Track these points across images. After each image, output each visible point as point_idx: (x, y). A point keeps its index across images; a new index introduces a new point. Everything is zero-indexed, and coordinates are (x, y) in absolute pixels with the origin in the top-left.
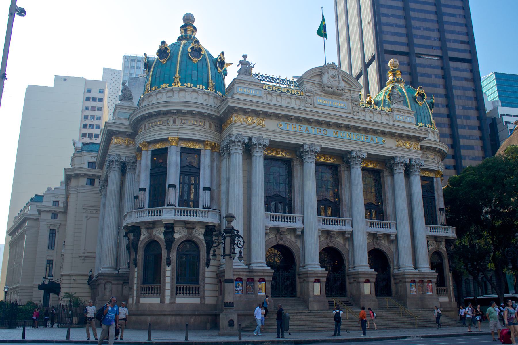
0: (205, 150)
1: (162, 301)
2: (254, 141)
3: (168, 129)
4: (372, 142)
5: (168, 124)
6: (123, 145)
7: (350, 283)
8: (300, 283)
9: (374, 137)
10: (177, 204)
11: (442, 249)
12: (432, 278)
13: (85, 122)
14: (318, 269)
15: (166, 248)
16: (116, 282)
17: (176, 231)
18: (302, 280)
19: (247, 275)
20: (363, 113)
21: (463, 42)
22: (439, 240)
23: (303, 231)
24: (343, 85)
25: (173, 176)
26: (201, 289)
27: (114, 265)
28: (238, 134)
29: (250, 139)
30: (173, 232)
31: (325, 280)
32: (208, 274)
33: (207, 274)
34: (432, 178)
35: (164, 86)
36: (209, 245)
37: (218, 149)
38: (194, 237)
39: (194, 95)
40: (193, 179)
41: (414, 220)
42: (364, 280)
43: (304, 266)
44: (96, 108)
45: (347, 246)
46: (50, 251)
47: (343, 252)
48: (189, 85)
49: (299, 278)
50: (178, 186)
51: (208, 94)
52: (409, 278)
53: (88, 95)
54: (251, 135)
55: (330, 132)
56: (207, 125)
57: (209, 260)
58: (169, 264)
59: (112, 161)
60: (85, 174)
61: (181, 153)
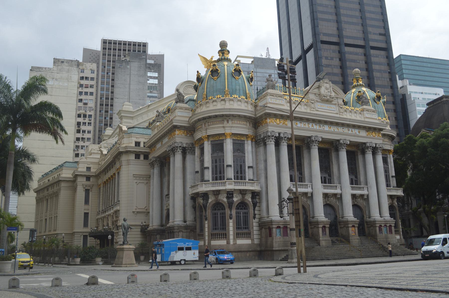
0: (247, 140)
1: (228, 243)
2: (282, 135)
3: (224, 127)
5: (223, 123)
6: (183, 135)
7: (341, 228)
8: (311, 228)
9: (353, 130)
10: (233, 178)
12: (392, 223)
13: (80, 98)
14: (323, 219)
15: (229, 207)
16: (185, 231)
17: (234, 196)
18: (313, 227)
19: (283, 224)
20: (345, 113)
21: (380, 34)
22: (393, 197)
23: (312, 194)
24: (333, 94)
25: (229, 159)
26: (252, 234)
27: (182, 219)
28: (273, 131)
29: (279, 134)
30: (233, 197)
31: (328, 226)
32: (255, 224)
33: (255, 224)
35: (219, 96)
36: (255, 205)
37: (255, 140)
39: (239, 103)
41: (379, 185)
42: (351, 225)
43: (313, 217)
44: (89, 86)
45: (337, 203)
46: (87, 207)
47: (336, 207)
48: (235, 96)
49: (311, 225)
50: (233, 166)
51: (247, 102)
53: (82, 75)
54: (280, 131)
55: (326, 128)
56: (248, 124)
57: (255, 215)
58: (231, 218)
59: (177, 147)
60: (134, 151)
61: (233, 143)
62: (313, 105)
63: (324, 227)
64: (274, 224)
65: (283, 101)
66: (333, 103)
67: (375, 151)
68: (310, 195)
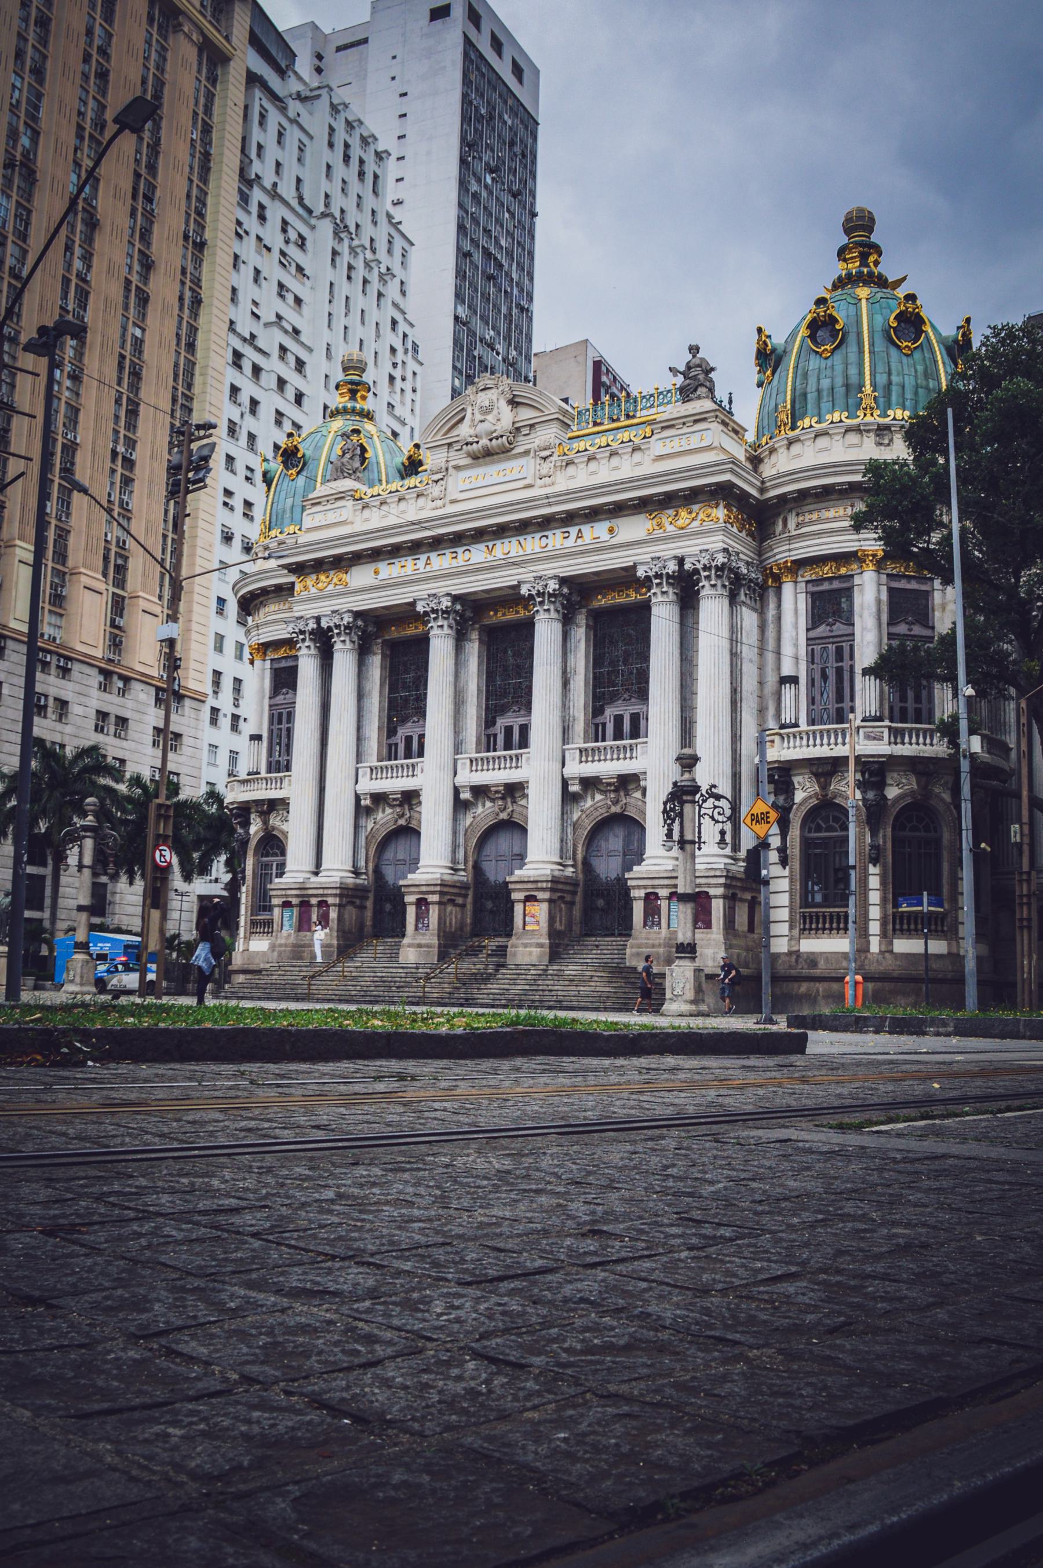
2: (324, 624)
4: (580, 542)
9: (586, 529)
11: (838, 794)
19: (297, 896)
34: (852, 576)
38: (274, 828)
50: (265, 735)
52: (639, 887)
54: (315, 613)
62: (436, 490)
63: (421, 903)
64: (277, 896)
65: (344, 511)
66: (514, 452)
67: (686, 587)
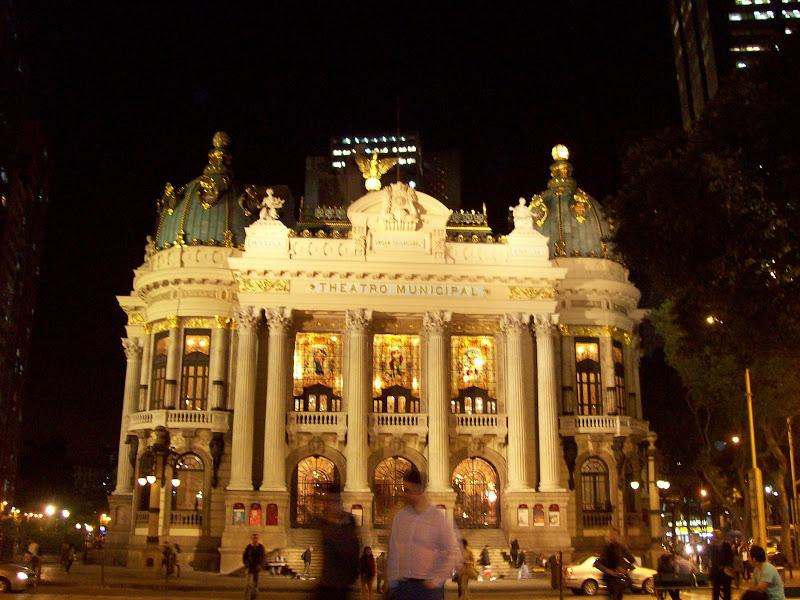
19: (249, 500)
31: (369, 505)
40: (200, 369)
68: (343, 439)
